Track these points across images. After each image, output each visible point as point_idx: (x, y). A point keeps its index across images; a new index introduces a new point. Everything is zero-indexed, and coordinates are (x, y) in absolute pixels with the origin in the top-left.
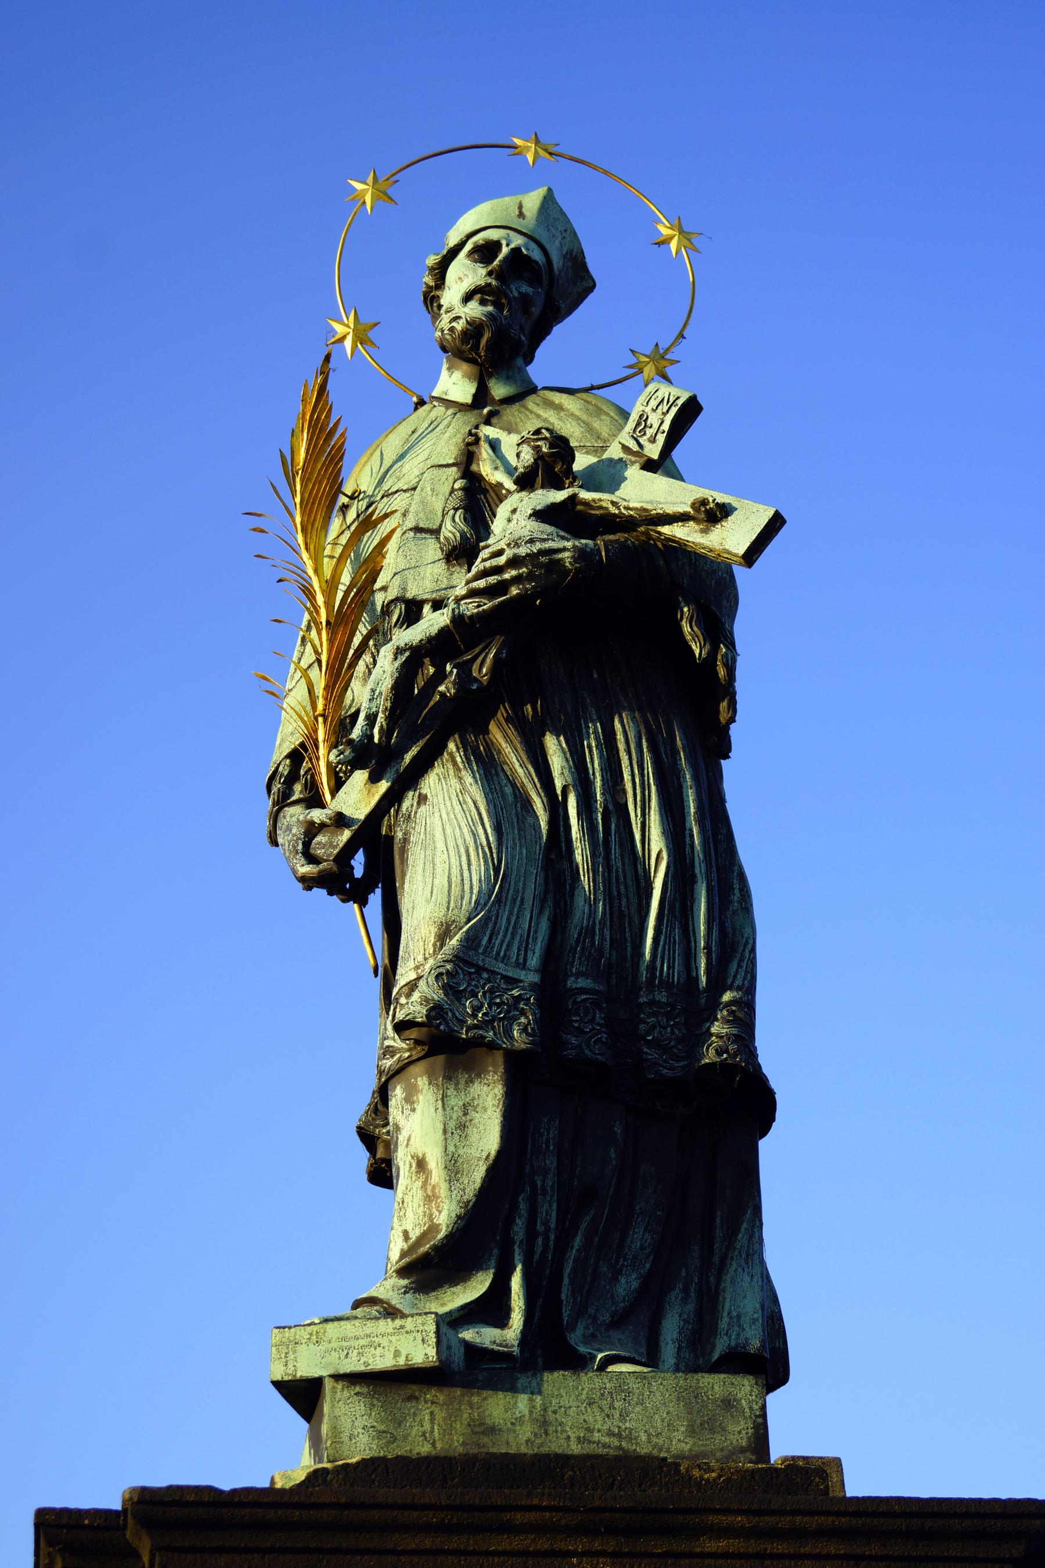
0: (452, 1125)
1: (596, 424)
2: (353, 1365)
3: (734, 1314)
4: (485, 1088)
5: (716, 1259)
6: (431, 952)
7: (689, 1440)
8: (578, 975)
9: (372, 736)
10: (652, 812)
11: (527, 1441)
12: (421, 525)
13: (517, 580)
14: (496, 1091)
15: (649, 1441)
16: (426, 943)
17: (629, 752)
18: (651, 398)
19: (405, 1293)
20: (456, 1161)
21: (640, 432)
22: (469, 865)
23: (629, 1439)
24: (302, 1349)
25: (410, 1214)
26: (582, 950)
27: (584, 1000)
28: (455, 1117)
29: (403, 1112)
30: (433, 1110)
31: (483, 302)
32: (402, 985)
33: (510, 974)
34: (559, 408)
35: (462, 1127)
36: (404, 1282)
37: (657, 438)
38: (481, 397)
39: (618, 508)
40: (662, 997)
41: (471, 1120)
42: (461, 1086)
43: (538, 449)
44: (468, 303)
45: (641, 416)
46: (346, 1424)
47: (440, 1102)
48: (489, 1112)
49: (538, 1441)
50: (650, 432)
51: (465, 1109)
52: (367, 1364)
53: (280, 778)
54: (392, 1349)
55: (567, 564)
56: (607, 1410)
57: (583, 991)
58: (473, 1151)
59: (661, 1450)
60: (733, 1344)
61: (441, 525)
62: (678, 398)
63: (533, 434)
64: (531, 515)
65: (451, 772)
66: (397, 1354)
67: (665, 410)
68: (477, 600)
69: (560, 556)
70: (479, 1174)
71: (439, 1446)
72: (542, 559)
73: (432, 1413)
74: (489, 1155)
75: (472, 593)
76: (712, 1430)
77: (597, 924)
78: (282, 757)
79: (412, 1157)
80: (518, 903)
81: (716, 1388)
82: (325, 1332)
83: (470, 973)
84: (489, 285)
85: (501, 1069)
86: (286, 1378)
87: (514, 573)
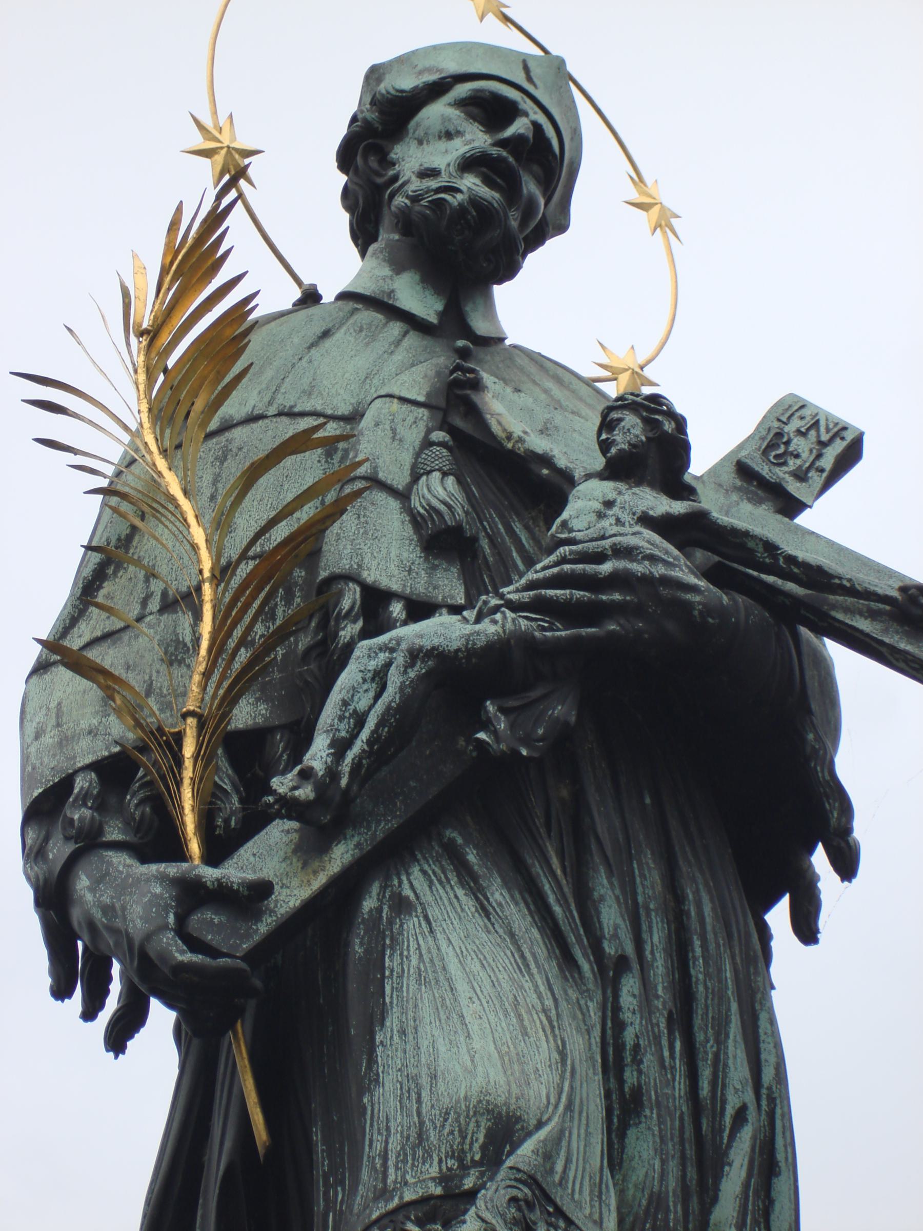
12: (381, 476)
16: (468, 1141)
18: (792, 415)
21: (776, 457)
31: (488, 182)
37: (810, 475)
39: (775, 557)
44: (466, 175)
45: (779, 435)
50: (793, 464)
55: (696, 613)
72: (664, 592)
77: (671, 1194)
80: (584, 1121)
83: (549, 1213)
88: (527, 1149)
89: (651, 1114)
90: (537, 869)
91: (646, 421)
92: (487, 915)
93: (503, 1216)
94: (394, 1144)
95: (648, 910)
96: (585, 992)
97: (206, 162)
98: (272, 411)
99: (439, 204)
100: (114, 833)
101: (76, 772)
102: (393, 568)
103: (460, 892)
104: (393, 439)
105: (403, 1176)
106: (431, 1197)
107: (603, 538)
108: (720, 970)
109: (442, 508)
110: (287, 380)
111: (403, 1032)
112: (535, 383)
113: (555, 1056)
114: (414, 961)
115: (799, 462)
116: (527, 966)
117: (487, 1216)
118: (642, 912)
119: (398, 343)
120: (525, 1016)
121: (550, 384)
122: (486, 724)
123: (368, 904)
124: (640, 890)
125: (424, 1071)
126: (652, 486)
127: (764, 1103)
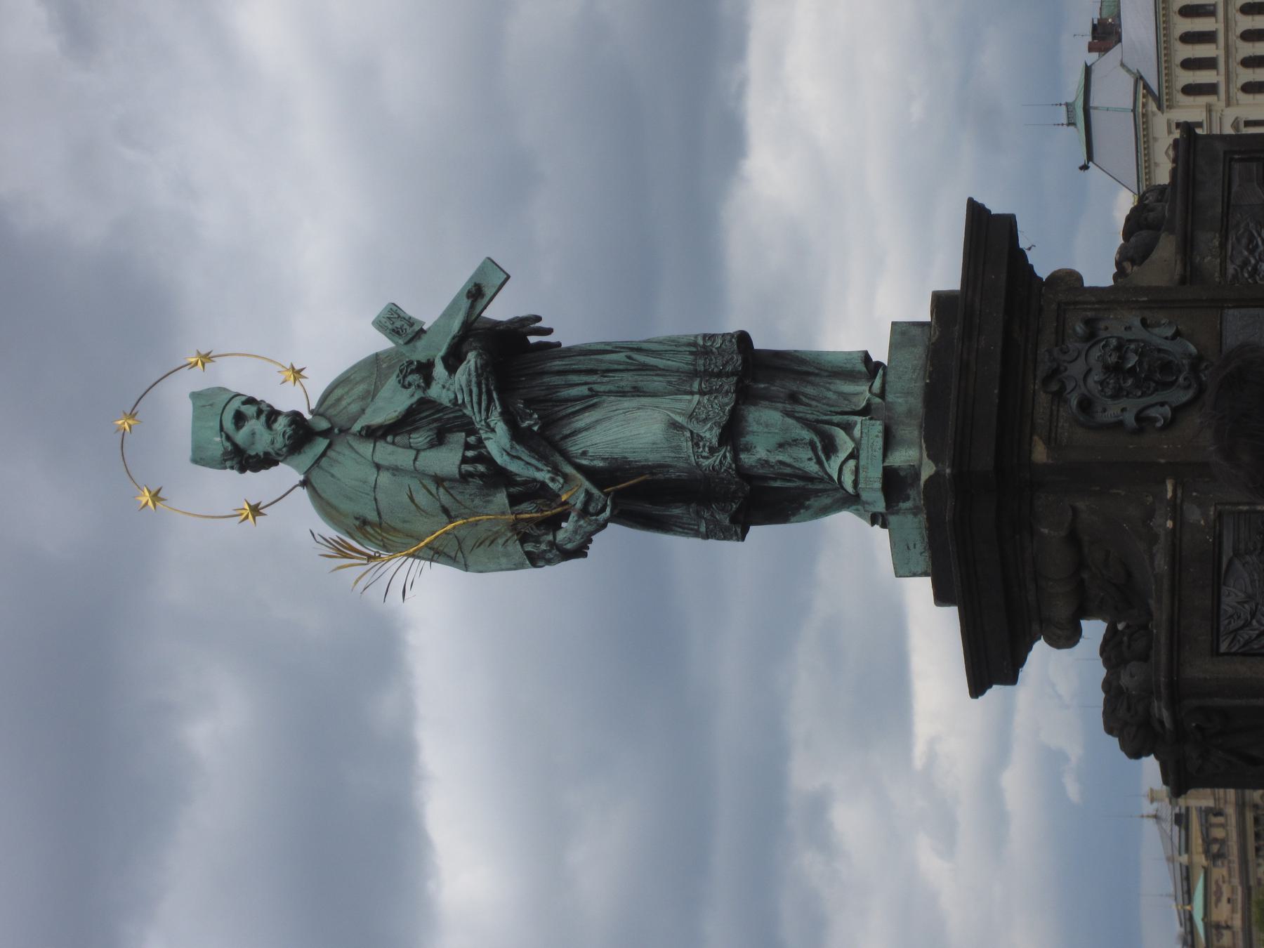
0: (766, 430)
1: (358, 379)
2: (879, 454)
4: (751, 415)
5: (817, 371)
8: (691, 386)
12: (413, 458)
13: (487, 385)
21: (403, 331)
26: (678, 384)
29: (754, 455)
30: (757, 437)
31: (275, 420)
32: (691, 451)
33: (696, 403)
34: (339, 400)
35: (767, 426)
36: (833, 457)
38: (325, 433)
40: (701, 362)
41: (765, 422)
43: (412, 372)
46: (903, 458)
48: (762, 414)
50: (406, 326)
51: (759, 423)
57: (700, 385)
58: (779, 423)
62: (391, 309)
65: (573, 438)
66: (877, 436)
67: (397, 316)
69: (479, 365)
70: (790, 421)
72: (480, 371)
73: (902, 430)
75: (487, 410)
87: (483, 386)
88: (680, 419)
89: (640, 384)
90: (564, 413)
91: (410, 373)
92: (589, 428)
93: (703, 426)
94: (673, 455)
96: (604, 401)
97: (257, 518)
100: (550, 537)
101: (523, 550)
103: (580, 436)
107: (462, 389)
108: (580, 360)
109: (428, 439)
111: (634, 452)
112: (344, 408)
113: (641, 410)
117: (704, 431)
119: (339, 453)
121: (344, 403)
122: (530, 427)
123: (585, 462)
126: (432, 373)
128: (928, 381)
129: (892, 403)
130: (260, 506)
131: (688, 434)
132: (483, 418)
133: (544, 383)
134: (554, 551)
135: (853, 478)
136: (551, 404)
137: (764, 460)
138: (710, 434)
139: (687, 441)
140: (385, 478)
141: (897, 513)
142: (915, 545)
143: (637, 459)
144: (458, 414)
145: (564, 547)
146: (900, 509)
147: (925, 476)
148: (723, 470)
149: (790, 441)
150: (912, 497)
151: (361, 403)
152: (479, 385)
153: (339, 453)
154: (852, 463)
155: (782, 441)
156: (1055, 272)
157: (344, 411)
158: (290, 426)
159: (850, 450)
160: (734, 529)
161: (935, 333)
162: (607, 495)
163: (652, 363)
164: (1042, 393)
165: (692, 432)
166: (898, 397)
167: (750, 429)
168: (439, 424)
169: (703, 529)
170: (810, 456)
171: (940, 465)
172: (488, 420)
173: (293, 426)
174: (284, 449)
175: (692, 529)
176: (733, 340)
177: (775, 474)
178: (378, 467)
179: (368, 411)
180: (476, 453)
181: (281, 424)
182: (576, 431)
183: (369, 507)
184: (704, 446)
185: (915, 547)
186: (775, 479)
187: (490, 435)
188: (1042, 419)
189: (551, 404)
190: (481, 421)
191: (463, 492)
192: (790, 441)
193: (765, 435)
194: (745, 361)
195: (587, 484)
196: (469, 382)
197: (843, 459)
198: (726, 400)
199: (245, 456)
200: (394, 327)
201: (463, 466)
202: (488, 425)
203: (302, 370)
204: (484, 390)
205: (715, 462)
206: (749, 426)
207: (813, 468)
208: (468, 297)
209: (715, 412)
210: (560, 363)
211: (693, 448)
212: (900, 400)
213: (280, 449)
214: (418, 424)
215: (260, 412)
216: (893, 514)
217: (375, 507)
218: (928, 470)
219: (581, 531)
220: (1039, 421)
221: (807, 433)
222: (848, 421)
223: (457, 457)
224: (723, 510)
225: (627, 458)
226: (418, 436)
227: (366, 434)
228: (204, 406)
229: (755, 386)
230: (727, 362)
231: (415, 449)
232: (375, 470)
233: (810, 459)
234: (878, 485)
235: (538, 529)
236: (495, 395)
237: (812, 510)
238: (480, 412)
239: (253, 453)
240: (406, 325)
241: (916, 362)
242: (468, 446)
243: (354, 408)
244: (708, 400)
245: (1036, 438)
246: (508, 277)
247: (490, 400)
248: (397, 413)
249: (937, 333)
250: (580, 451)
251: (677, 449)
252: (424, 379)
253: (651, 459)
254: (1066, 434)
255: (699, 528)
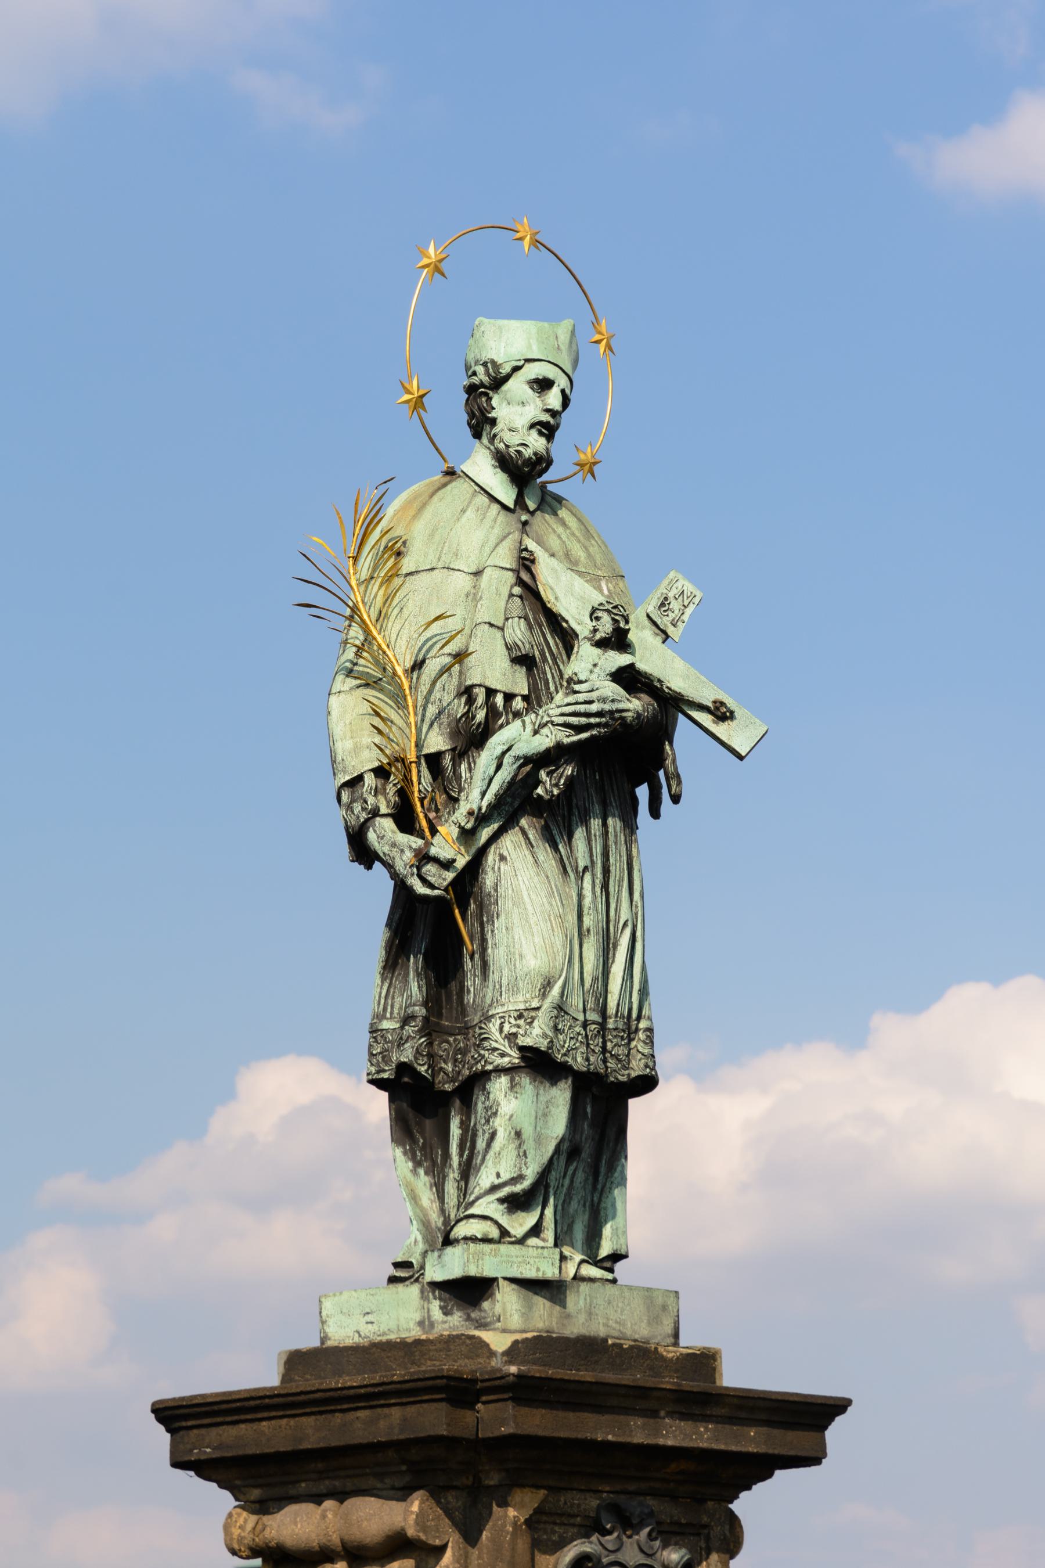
0: (540, 1113)
1: (591, 549)
3: (615, 1227)
4: (559, 1092)
5: (599, 1187)
6: (537, 994)
7: (647, 1328)
9: (480, 809)
10: (624, 889)
11: (583, 1323)
13: (598, 725)
14: (565, 1095)
15: (631, 1326)
17: (616, 843)
19: (503, 1215)
20: (540, 1137)
21: (665, 611)
22: (553, 931)
23: (624, 1325)
24: (487, 1258)
25: (503, 1162)
26: (593, 991)
27: (595, 1029)
28: (542, 1109)
29: (506, 1096)
30: (530, 1102)
31: (541, 433)
32: (510, 1008)
33: (575, 1016)
34: (563, 523)
35: (545, 1115)
37: (678, 624)
39: (662, 685)
41: (550, 1112)
42: (547, 1089)
43: (615, 621)
45: (666, 599)
46: (508, 1306)
47: (535, 1097)
48: (561, 1108)
49: (587, 1324)
50: (672, 616)
51: (548, 1103)
52: (521, 1273)
53: (371, 789)
54: (536, 1267)
55: (628, 721)
56: (615, 1308)
57: (594, 1023)
58: (549, 1132)
59: (636, 1333)
60: (615, 1248)
61: (504, 624)
62: (695, 596)
63: (613, 608)
64: (608, 674)
66: (538, 1270)
67: (686, 604)
68: (568, 730)
69: (624, 714)
71: (547, 1324)
72: (617, 715)
73: (544, 1304)
74: (558, 1136)
75: (566, 725)
76: (657, 1323)
78: (366, 769)
79: (512, 1128)
81: (660, 1298)
82: (499, 1250)
84: (548, 423)
85: (570, 1081)
86: (478, 1275)
87: (597, 720)
90: (555, 832)
91: (613, 619)
94: (504, 982)
95: (595, 836)
97: (407, 405)
98: (440, 565)
99: (518, 452)
100: (384, 810)
102: (498, 675)
103: (527, 852)
104: (496, 594)
105: (509, 998)
106: (519, 1010)
107: (592, 691)
109: (520, 643)
110: (446, 544)
112: (554, 531)
113: (564, 938)
114: (510, 892)
115: (674, 615)
116: (553, 892)
117: (543, 1026)
118: (593, 838)
120: (553, 922)
121: (560, 530)
124: (593, 828)
125: (517, 952)
126: (612, 649)
127: (634, 908)
128: (610, 1342)
129: (578, 1291)
130: (421, 411)
131: (535, 1004)
132: (553, 719)
133: (593, 804)
134: (364, 816)
135: (479, 1236)
136: (566, 813)
137: (497, 1110)
138: (535, 1036)
139: (526, 1002)
140: (463, 582)
141: (423, 1296)
142: (372, 1323)
143: (496, 932)
144: (551, 685)
145: (371, 829)
146: (429, 1302)
147: (486, 1336)
148: (482, 1052)
149: (525, 1148)
150: (449, 1318)
151: (561, 554)
152: (599, 714)
153: (495, 520)
154: (495, 1233)
155: (524, 1136)
156: (739, 1521)
157: (550, 530)
158: (535, 454)
159: (512, 1232)
160: (387, 1068)
161: (668, 1352)
162: (446, 890)
163: (617, 955)
164: (598, 1502)
165: (538, 1009)
166: (585, 1299)
167: (541, 1092)
168: (537, 659)
169: (386, 1025)
170: (502, 1175)
171: (505, 1358)
172: (550, 725)
173: (534, 457)
174: (502, 446)
175: (385, 1009)
176: (648, 1070)
177: (475, 1124)
178: (478, 573)
179: (553, 562)
180: (501, 709)
181: (536, 443)
182: (532, 847)
183: (421, 560)
184: (519, 1027)
185: (367, 1323)
186: (464, 1125)
187: (529, 728)
188: (565, 1503)
189: (566, 813)
190: (548, 715)
191: (444, 690)
192: (525, 1147)
193: (533, 1113)
194: (621, 1084)
195: (461, 862)
196: (604, 700)
197: (500, 1222)
198: (579, 1059)
199: (491, 393)
200: (671, 599)
201: (483, 690)
202: (545, 725)
203: (593, 476)
204: (592, 720)
205: (496, 1041)
206: (544, 1090)
207: (485, 1178)
208: (715, 702)
209: (565, 1042)
210: (618, 829)
211: (516, 1010)
212: (582, 1303)
213: (502, 440)
214: (536, 629)
215: (554, 413)
216: (422, 1292)
217: (420, 569)
218: (498, 1342)
219: (395, 852)
220: (562, 1499)
221: (535, 1172)
222: (548, 1230)
223: (495, 682)
224: (418, 1053)
225: (498, 918)
226: (523, 629)
227: (524, 558)
228: (557, 337)
229: (588, 1100)
230: (620, 1061)
231: (504, 624)
232: (473, 569)
233: (498, 1175)
234: (473, 1271)
235: (396, 791)
236: (584, 736)
237: (412, 1179)
238: (562, 715)
239: (494, 403)
240: (674, 615)
241: (629, 1325)
242: (509, 697)
243: (554, 543)
244: (579, 1034)
245: (542, 1493)
246: (741, 758)
247: (578, 729)
248: (553, 600)
249: (670, 1355)
250: (505, 853)
251: (514, 988)
252: (605, 638)
253: (496, 951)
254: (545, 1537)
255: (388, 1019)
